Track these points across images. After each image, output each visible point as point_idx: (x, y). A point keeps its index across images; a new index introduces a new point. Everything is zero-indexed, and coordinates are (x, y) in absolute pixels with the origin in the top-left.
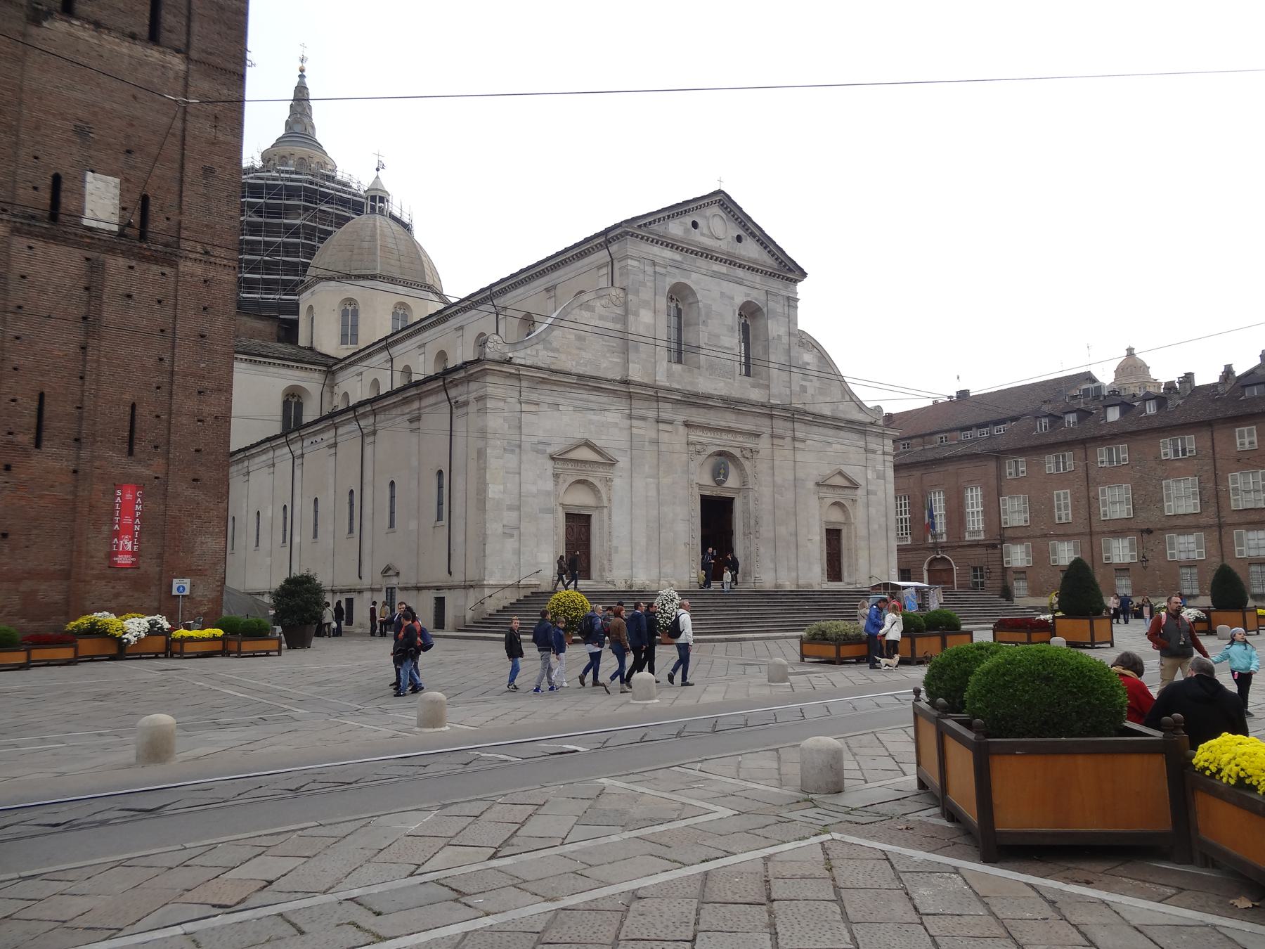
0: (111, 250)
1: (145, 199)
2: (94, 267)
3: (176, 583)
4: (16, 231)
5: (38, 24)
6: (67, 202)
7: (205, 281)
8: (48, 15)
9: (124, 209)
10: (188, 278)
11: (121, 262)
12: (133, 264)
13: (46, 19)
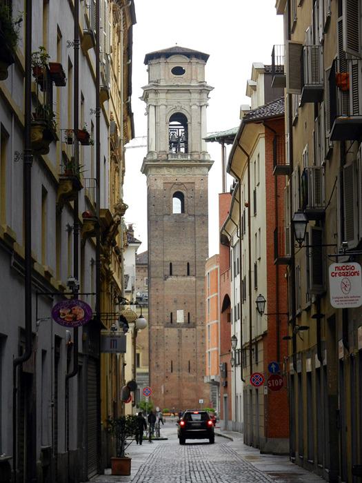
0: (182, 327)
1: (189, 314)
2: (180, 332)
4: (165, 327)
5: (165, 279)
6: (173, 318)
8: (168, 277)
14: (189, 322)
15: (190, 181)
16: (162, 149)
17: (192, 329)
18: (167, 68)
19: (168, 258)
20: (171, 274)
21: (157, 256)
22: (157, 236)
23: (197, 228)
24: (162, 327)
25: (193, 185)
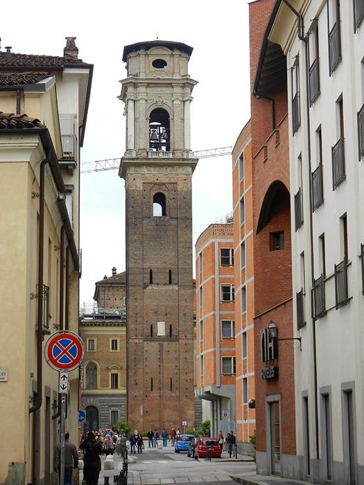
0: (164, 341)
1: (171, 326)
2: (161, 346)
3: (183, 422)
4: (144, 341)
5: (145, 288)
8: (148, 286)
15: (172, 181)
16: (142, 147)
17: (174, 343)
18: (147, 61)
19: (147, 265)
20: (151, 282)
21: (135, 262)
22: (135, 241)
23: (179, 232)
24: (141, 341)
25: (175, 185)
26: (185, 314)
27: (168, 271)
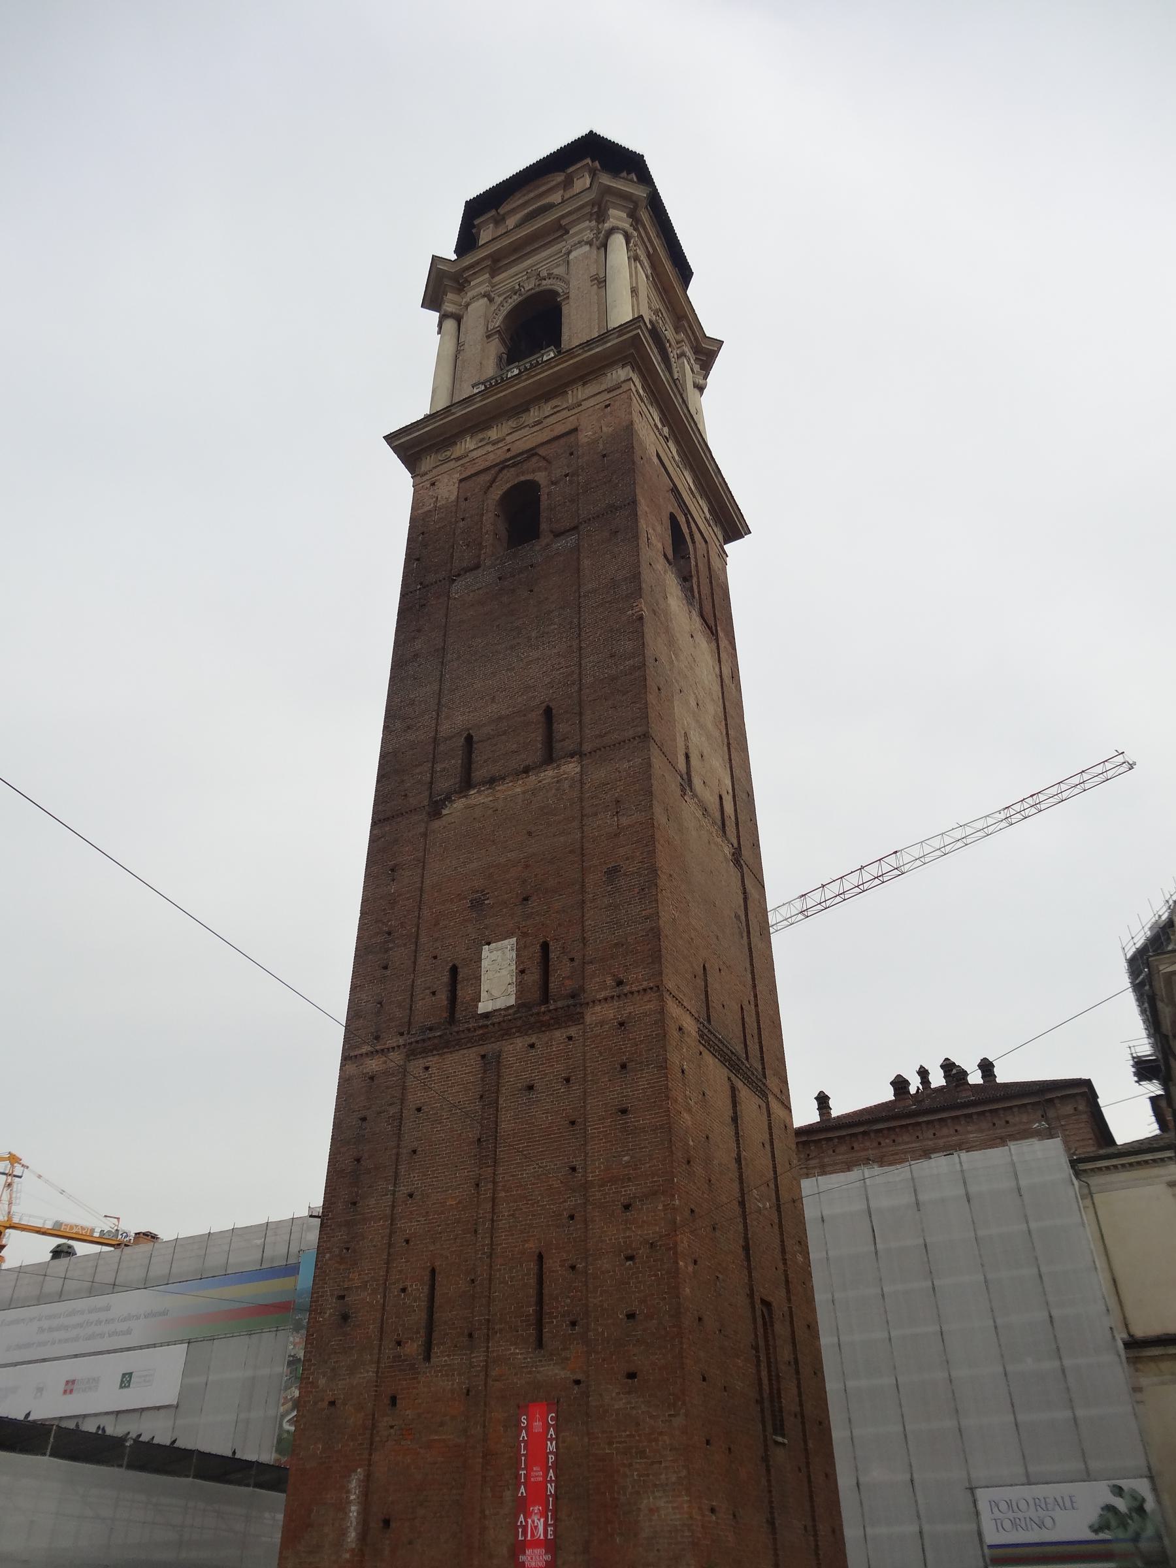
1: (545, 947)
2: (491, 1064)
6: (463, 993)
7: (622, 1024)
9: (522, 972)
10: (598, 1030)
11: (520, 1043)
12: (533, 1040)
13: (444, 806)
14: (545, 997)
17: (559, 1035)
24: (396, 1057)
26: (613, 873)
27: (536, 716)
